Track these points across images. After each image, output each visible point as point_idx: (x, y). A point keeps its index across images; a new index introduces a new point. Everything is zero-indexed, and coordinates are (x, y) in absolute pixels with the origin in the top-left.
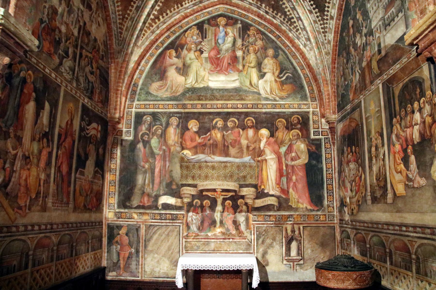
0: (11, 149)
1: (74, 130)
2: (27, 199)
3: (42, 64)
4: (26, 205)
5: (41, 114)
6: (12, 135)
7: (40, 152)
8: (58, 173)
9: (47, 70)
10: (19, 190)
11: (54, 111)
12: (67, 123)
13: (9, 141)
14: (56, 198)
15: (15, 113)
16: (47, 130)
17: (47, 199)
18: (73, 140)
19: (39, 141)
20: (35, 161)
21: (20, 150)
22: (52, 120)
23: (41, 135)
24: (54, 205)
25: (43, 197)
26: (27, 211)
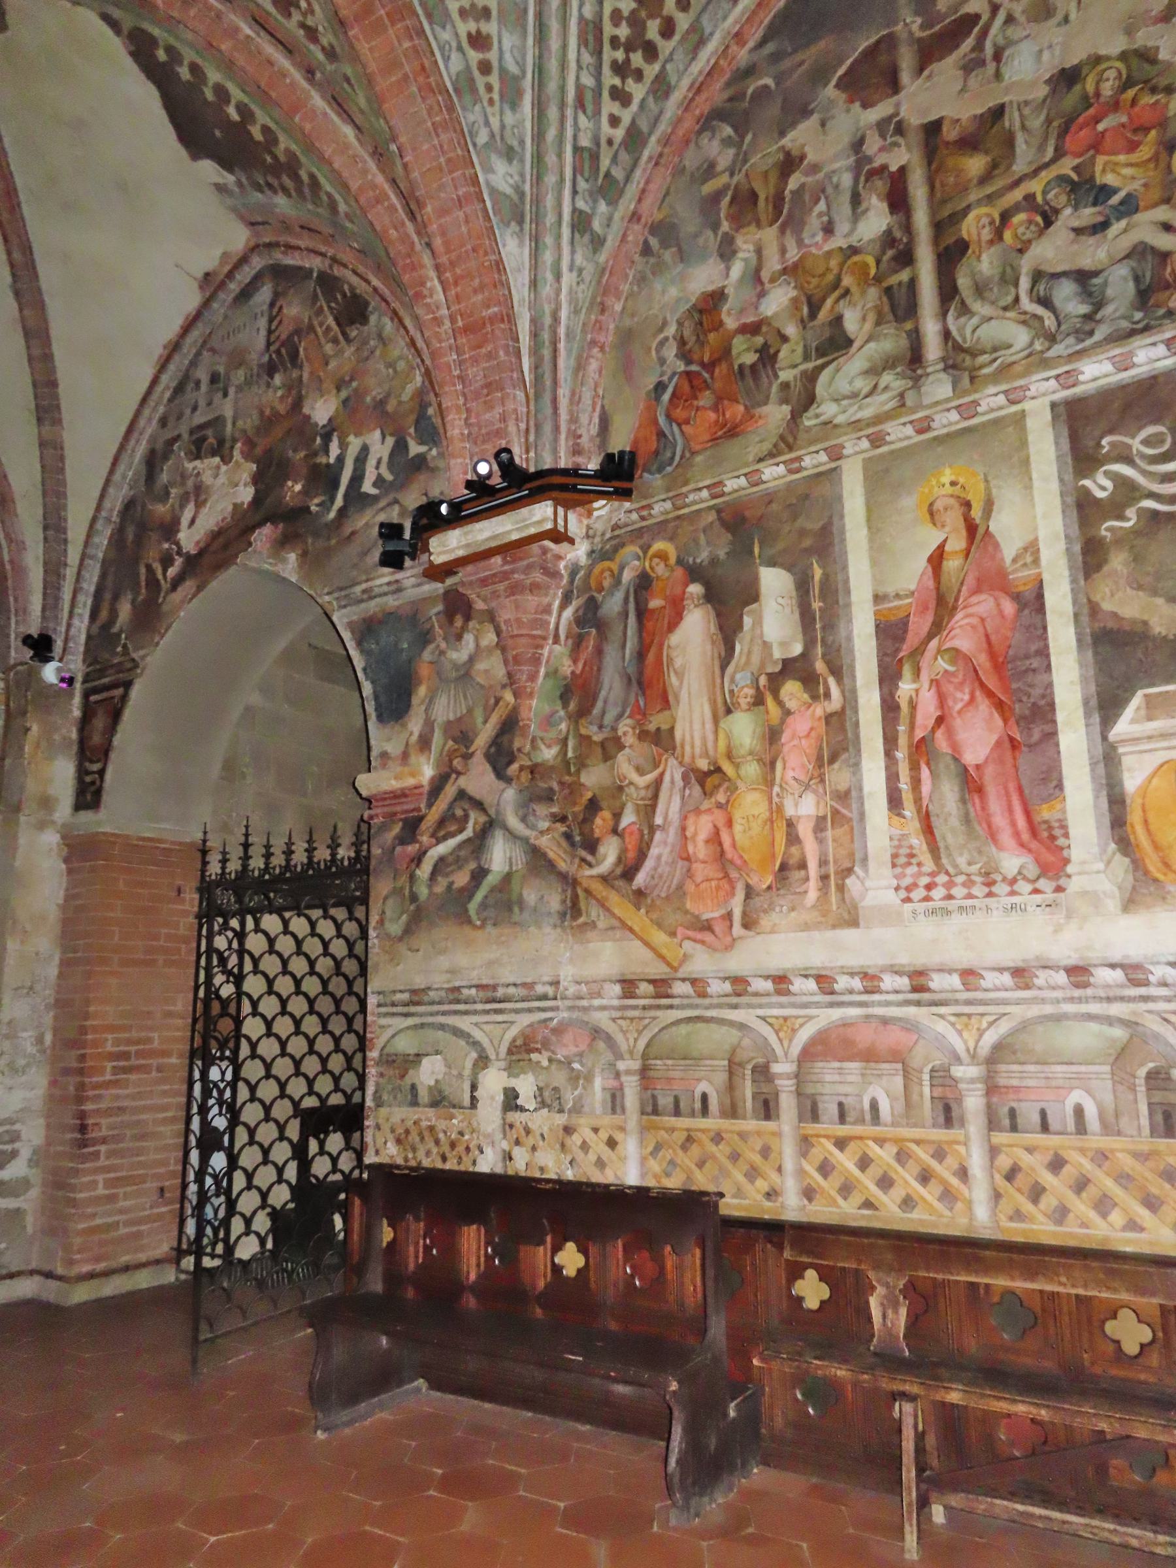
0: (634, 776)
1: (1009, 551)
2: (732, 893)
3: (700, 489)
4: (729, 916)
5: (747, 621)
6: (630, 740)
7: (773, 735)
8: (915, 768)
9: (731, 485)
10: (689, 874)
11: (818, 573)
12: (937, 559)
13: (621, 757)
14: (929, 866)
15: (630, 679)
16: (797, 649)
17: (850, 882)
18: (1017, 597)
19: (759, 701)
20: (751, 769)
21: (673, 762)
22: (816, 605)
23: (763, 680)
24: (917, 894)
25: (824, 878)
26: (737, 929)
